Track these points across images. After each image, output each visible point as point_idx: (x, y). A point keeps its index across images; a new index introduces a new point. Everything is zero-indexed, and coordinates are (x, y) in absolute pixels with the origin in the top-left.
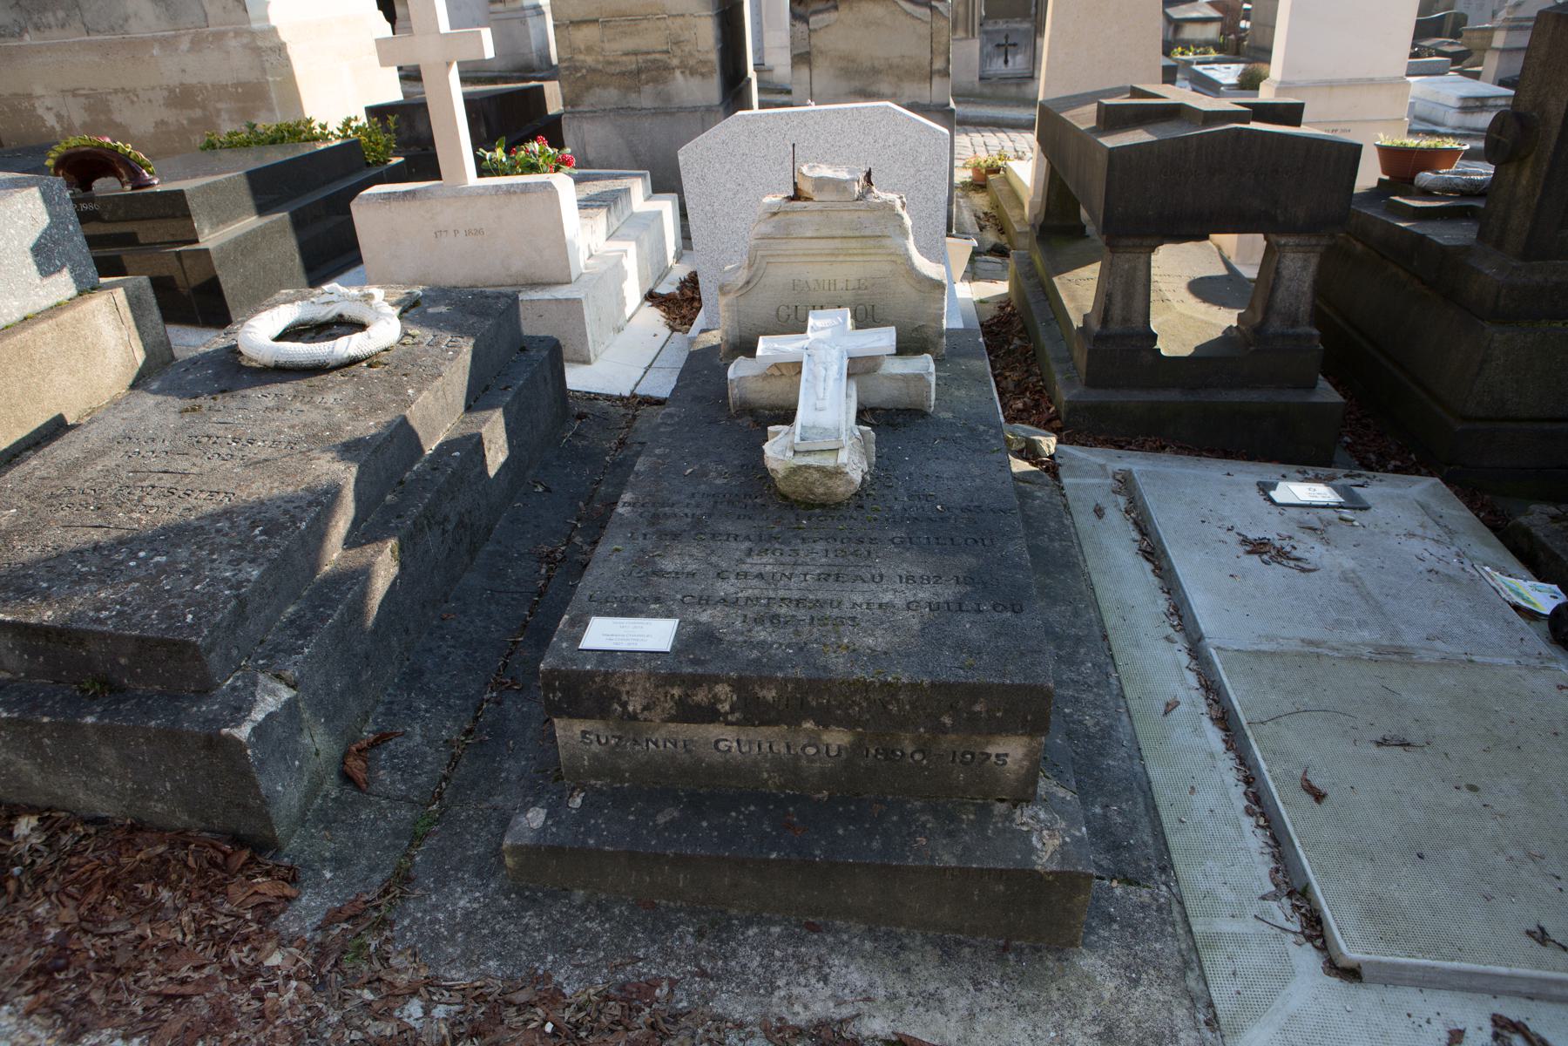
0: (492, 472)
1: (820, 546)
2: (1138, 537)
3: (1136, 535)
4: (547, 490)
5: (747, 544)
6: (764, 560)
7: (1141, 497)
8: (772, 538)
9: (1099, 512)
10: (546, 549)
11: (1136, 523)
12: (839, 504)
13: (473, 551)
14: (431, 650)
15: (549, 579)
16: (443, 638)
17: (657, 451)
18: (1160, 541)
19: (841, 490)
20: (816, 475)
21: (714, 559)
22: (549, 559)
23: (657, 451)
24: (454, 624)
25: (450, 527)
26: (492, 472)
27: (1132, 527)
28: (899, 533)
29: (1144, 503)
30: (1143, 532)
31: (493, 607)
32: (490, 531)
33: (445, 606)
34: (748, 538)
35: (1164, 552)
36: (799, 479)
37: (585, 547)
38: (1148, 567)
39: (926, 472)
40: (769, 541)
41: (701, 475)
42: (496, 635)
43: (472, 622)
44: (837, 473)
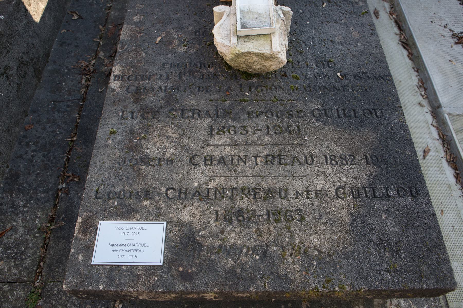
0: (37, 18)
1: (262, 122)
2: (398, 32)
3: (396, 30)
4: (80, 17)
5: (208, 122)
6: (223, 141)
7: (399, 4)
8: (227, 113)
9: (376, 14)
10: (84, 64)
11: (396, 22)
12: (270, 73)
13: (38, 73)
14: (21, 157)
15: (87, 87)
16: (28, 145)
17: (136, 19)
18: (411, 36)
19: (273, 66)
20: (255, 59)
21: (185, 141)
22: (85, 72)
23: (136, 19)
24: (34, 132)
25: (13, 71)
26: (37, 18)
27: (394, 25)
28: (315, 105)
29: (401, 9)
30: (400, 28)
31: (56, 115)
32: (47, 55)
33: (27, 119)
34: (208, 114)
35: (414, 44)
36: (242, 60)
37: (106, 61)
38: (405, 53)
39: (323, 36)
40: (224, 117)
41: (167, 42)
42: (60, 137)
43: (44, 129)
44: (272, 57)
